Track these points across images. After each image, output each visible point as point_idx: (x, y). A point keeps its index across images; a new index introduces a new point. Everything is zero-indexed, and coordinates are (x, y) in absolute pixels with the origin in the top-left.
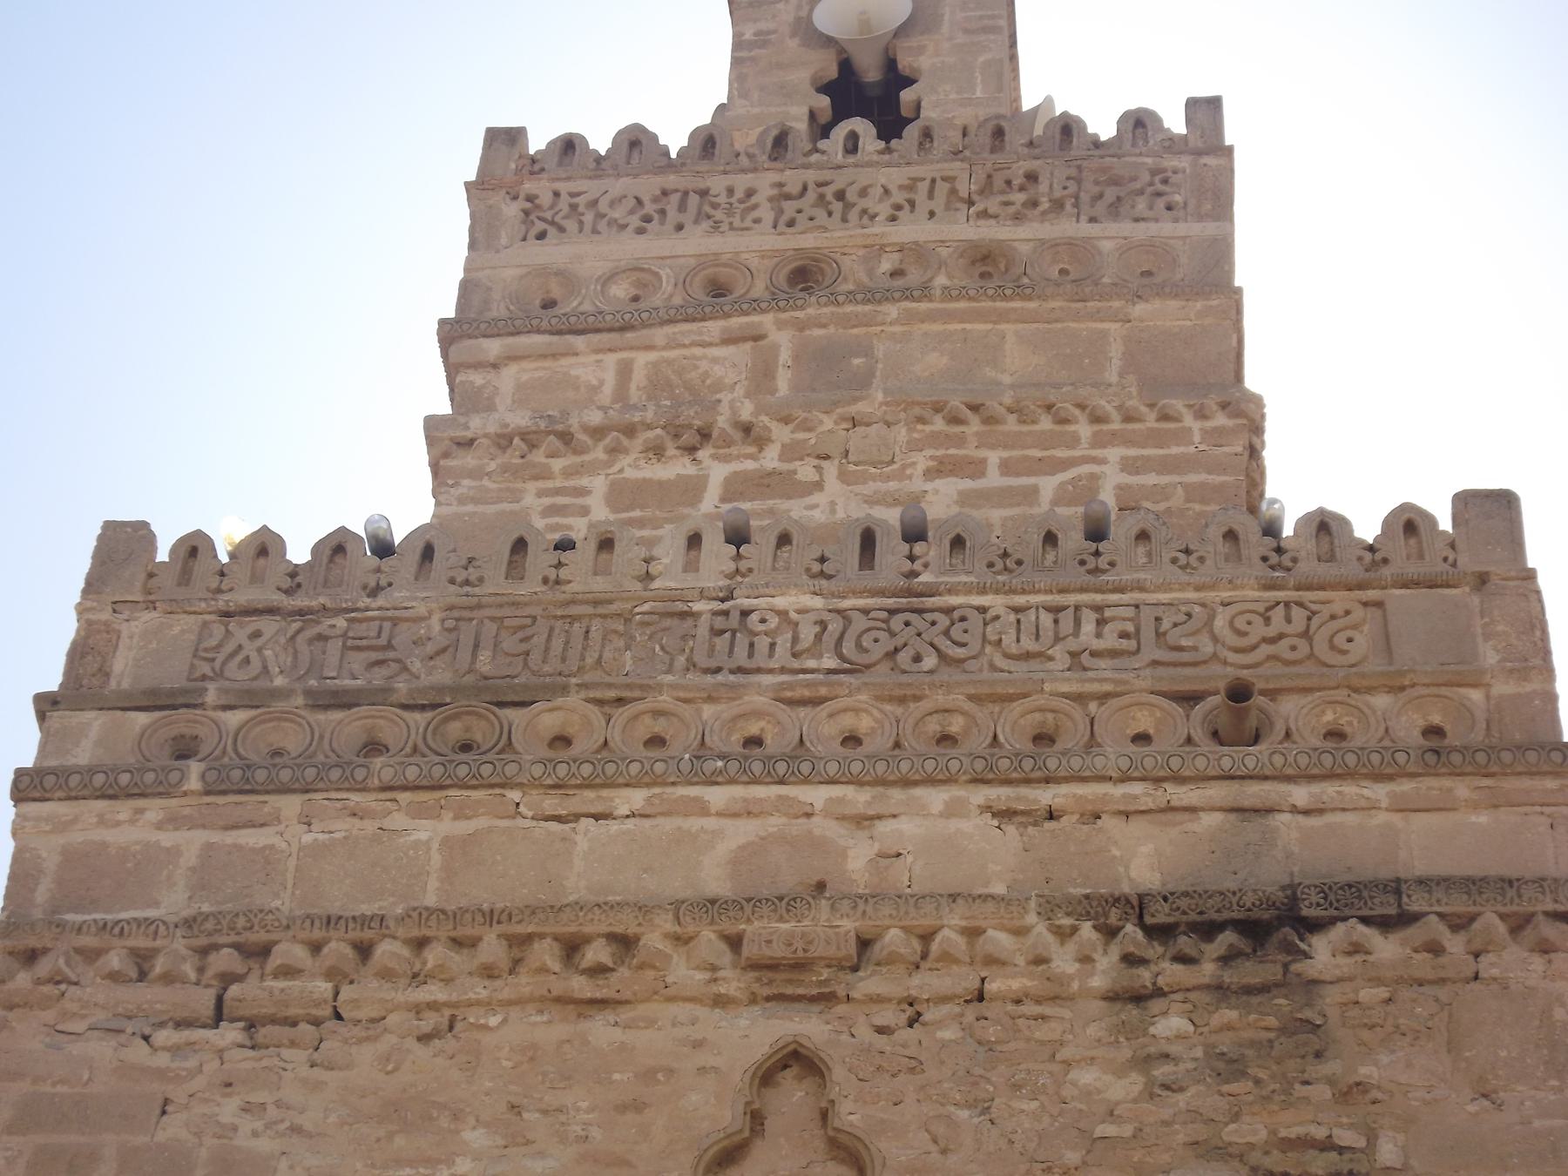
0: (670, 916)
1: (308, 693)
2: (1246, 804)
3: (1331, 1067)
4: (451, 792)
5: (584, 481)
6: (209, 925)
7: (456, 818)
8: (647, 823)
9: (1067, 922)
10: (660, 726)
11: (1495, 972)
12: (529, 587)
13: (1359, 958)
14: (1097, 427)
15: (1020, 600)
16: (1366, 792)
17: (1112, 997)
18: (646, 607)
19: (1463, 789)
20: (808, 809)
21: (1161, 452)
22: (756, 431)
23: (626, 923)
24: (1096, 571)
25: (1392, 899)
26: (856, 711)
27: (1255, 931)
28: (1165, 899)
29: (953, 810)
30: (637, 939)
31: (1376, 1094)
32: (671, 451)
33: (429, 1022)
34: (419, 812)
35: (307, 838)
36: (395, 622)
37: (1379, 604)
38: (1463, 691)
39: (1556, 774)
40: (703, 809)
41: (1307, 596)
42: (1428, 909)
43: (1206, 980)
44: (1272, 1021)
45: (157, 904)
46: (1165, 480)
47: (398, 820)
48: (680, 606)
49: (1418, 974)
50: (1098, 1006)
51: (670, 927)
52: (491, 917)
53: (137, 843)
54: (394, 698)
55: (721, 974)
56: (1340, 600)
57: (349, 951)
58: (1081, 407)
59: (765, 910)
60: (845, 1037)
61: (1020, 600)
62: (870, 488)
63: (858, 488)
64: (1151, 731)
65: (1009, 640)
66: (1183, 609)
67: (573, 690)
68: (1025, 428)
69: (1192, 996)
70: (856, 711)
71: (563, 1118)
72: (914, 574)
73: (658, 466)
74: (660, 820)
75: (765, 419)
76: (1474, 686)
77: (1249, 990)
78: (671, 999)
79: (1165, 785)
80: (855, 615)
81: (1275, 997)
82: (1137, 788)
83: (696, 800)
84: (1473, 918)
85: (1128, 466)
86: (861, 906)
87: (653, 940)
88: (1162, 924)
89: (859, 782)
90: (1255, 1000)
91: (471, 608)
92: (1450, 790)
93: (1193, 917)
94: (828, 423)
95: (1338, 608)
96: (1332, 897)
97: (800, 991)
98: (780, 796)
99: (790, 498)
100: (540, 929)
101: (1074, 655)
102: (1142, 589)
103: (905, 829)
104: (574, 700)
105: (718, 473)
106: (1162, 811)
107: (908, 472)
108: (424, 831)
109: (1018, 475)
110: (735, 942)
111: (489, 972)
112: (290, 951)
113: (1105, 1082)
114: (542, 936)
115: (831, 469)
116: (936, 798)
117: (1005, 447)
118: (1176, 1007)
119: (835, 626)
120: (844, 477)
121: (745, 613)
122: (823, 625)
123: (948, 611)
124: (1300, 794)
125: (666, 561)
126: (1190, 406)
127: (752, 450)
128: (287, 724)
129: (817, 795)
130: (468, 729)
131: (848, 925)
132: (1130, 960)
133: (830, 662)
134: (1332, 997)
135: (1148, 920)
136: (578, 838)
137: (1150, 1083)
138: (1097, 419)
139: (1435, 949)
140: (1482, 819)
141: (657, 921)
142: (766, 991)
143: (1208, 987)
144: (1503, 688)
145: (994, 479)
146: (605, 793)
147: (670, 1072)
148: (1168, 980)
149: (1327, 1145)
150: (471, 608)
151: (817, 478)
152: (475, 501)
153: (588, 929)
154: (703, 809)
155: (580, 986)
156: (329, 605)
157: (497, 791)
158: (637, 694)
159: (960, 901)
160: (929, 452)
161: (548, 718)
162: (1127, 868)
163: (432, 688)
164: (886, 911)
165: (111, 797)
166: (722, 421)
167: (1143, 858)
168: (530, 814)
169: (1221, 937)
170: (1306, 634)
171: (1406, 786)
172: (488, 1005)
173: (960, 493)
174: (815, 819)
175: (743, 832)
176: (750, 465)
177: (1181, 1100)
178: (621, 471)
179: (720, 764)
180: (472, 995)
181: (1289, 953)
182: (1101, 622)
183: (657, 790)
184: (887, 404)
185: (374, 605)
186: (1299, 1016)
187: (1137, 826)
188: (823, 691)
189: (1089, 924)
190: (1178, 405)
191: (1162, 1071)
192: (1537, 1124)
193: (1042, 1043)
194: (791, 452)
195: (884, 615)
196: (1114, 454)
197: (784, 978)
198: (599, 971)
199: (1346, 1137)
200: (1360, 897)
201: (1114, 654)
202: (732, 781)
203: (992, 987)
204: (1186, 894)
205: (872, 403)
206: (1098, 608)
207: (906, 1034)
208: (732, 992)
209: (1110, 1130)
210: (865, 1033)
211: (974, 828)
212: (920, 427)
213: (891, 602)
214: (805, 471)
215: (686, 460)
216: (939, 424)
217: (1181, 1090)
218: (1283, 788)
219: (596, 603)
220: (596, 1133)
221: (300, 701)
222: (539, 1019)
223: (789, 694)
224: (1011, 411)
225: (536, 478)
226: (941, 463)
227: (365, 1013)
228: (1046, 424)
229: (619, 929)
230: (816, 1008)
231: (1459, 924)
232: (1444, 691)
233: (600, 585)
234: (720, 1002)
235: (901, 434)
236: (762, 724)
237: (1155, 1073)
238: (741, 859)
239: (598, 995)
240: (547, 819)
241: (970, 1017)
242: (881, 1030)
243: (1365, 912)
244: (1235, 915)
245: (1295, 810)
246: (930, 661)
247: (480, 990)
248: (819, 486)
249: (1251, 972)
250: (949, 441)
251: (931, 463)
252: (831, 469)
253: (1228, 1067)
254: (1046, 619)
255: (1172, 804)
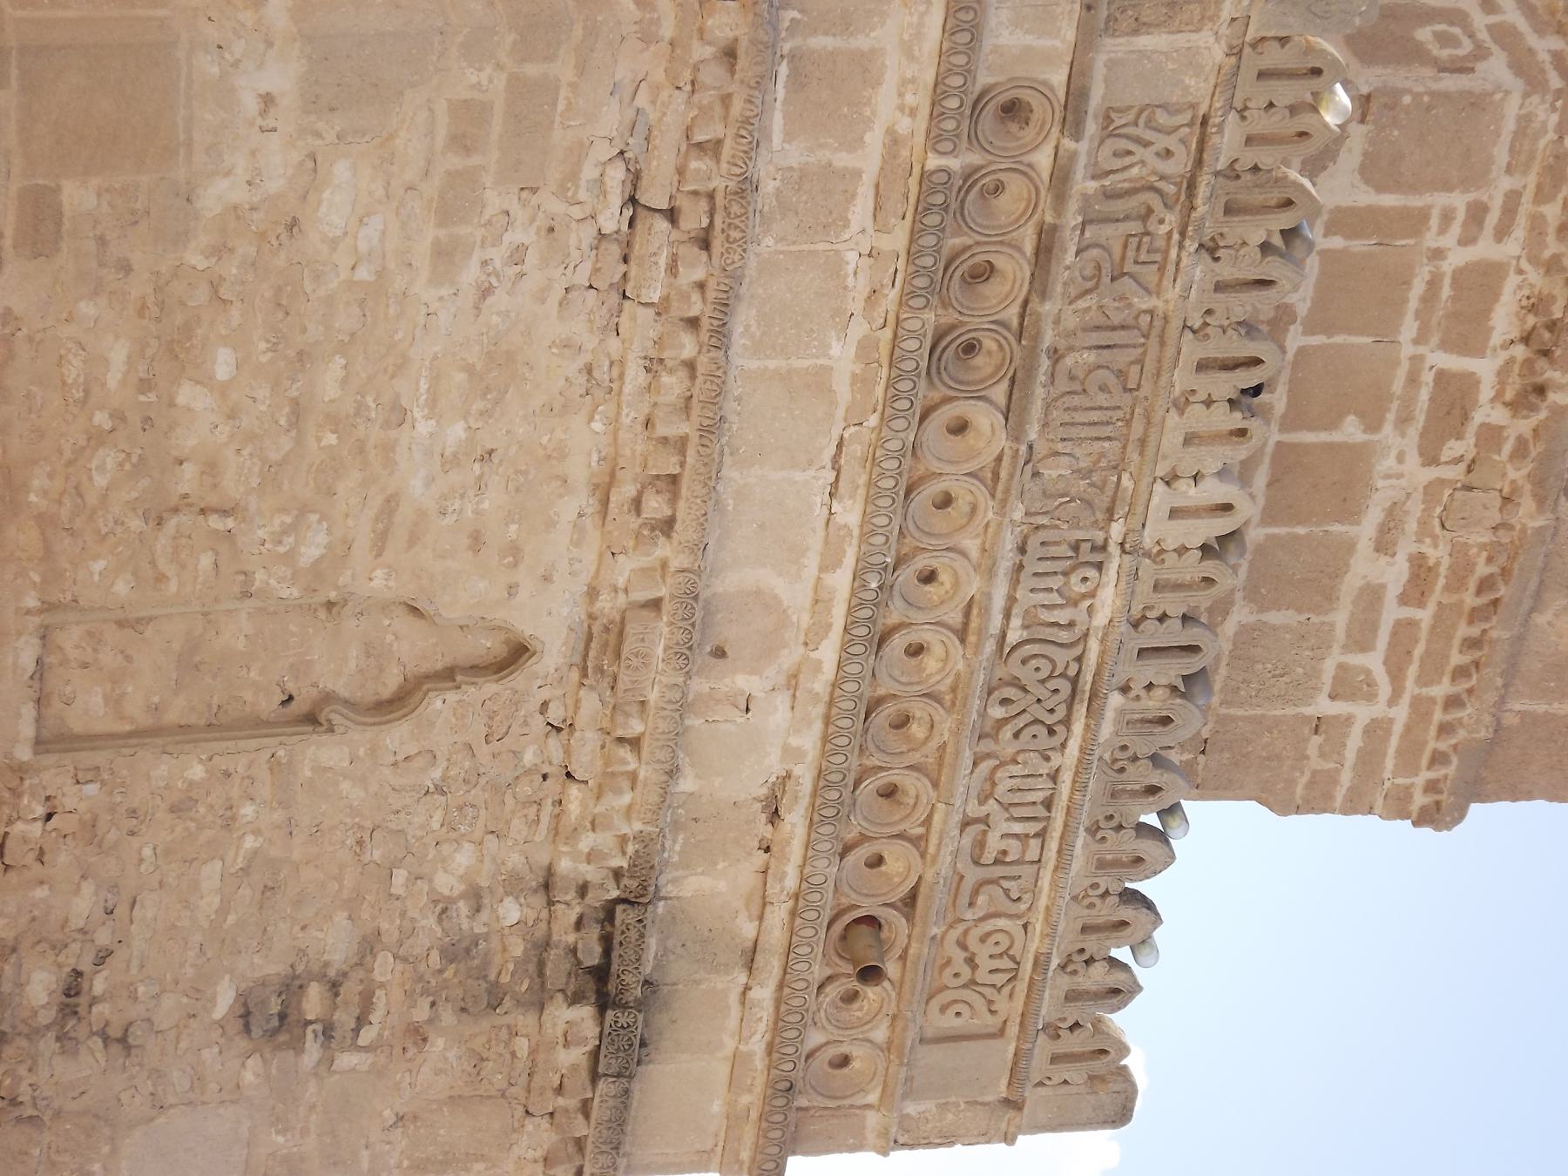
0: (686, 565)
1: (1054, 229)
2: (758, 957)
3: (448, 1017)
4: (884, 372)
5: (1520, 232)
6: (735, 209)
7: (854, 376)
8: (821, 523)
9: (630, 849)
10: (961, 506)
11: (530, 1128)
12: (1182, 378)
13: (561, 1040)
14: (1440, 701)
15: (1066, 778)
16: (758, 1037)
17: (550, 871)
18: (1126, 482)
19: (751, 1099)
20: (811, 647)
21: (1391, 751)
22: (1533, 398)
23: (684, 530)
24: (1094, 830)
25: (614, 1070)
26: (945, 660)
27: (601, 973)
28: (640, 921)
29: (790, 753)
30: (669, 536)
31: (412, 1051)
32: (1531, 320)
33: (601, 373)
34: (866, 348)
35: (852, 257)
36: (1162, 269)
37: (1001, 1033)
38: (879, 1090)
39: (753, 1160)
40: (829, 563)
41: (1022, 987)
42: (598, 1093)
43: (555, 937)
44: (505, 979)
45: (789, 137)
46: (1350, 754)
47: (859, 328)
48: (1120, 511)
49: (537, 1078)
50: (543, 859)
51: (674, 564)
52: (711, 430)
53: (874, 113)
54: (1035, 298)
55: (622, 596)
56: (1011, 1007)
57: (693, 313)
58: (1470, 691)
59: (680, 637)
60: (539, 682)
61: (1066, 778)
62: (1416, 508)
63: (1418, 495)
64: (883, 868)
65: (1016, 770)
66: (1026, 897)
67: (1015, 446)
68: (1456, 643)
69: (543, 926)
70: (945, 660)
71: (471, 493)
72: (1125, 690)
73: (1514, 308)
74: (821, 533)
75: (1543, 415)
76: (881, 1098)
77: (541, 965)
78: (601, 555)
79: (791, 903)
80: (1077, 651)
81: (531, 978)
82: (791, 882)
83: (838, 563)
84: (587, 1116)
85: (1377, 730)
86: (670, 707)
87: (663, 549)
88: (628, 902)
89: (835, 685)
90: (532, 968)
91: (1162, 337)
92: (750, 1091)
93: (617, 938)
94: (1517, 474)
95: (1001, 1004)
96: (622, 1032)
97: (592, 654)
98: (830, 625)
99: (1422, 435)
100: (688, 466)
101: (985, 820)
102: (1056, 868)
103: (776, 715)
104: (1002, 441)
105: (1485, 368)
106: (764, 897)
107: (1428, 540)
108: (841, 355)
109: (1394, 634)
110: (655, 604)
111: (648, 423)
112: (695, 269)
113: (458, 865)
114: (682, 464)
115: (1456, 473)
116: (809, 741)
117: (1433, 627)
118: (532, 915)
119: (1064, 636)
120: (1442, 482)
121: (1099, 566)
122: (1071, 624)
123: (1067, 722)
124: (764, 994)
125: (1192, 491)
126: (1446, 777)
127: (1509, 395)
128: (1023, 206)
129: (828, 653)
130: (990, 353)
131: (653, 697)
132: (583, 890)
133: (1013, 637)
134: (525, 1020)
135: (619, 908)
136: (811, 473)
137: (453, 900)
138: (1453, 702)
139: (560, 1090)
140: (717, 1107)
141: (681, 556)
142: (596, 629)
143: (550, 936)
144: (872, 1119)
145: (1392, 612)
146: (862, 492)
147: (515, 565)
148: (559, 913)
149: (362, 1021)
150: (1162, 337)
151: (1443, 459)
152: (1520, 134)
153: (682, 505)
154: (829, 563)
155: (625, 491)
156: (1194, 215)
157: (880, 408)
158: (999, 495)
159: (665, 778)
160: (1446, 562)
161: (986, 420)
162: (702, 873)
163: (1038, 333)
164: (663, 726)
165: (936, 85)
166: (1552, 375)
167: (712, 887)
168: (846, 436)
169: (598, 949)
170: (973, 982)
171: (759, 1062)
172: (614, 422)
173: (1383, 586)
174: (802, 649)
175: (794, 595)
176: (1486, 392)
177: (430, 921)
178: (1520, 272)
179: (874, 585)
180: (625, 411)
181: (575, 993)
182: (1023, 838)
183: (856, 532)
184: (1524, 530)
185: (1184, 254)
186: (507, 998)
187: (755, 880)
188: (972, 638)
189: (625, 865)
190: (1451, 770)
191: (463, 908)
192: (365, 1154)
193: (508, 822)
194: (1491, 436)
195: (1072, 672)
196: (1401, 714)
197: (603, 647)
198: (637, 504)
199: (367, 1036)
200: (618, 1050)
201: (980, 844)
202: (853, 594)
203: (574, 791)
204: (642, 936)
205: (1527, 515)
206: (1042, 835)
207: (538, 723)
208: (598, 605)
209: (400, 876)
210: (545, 694)
211: (774, 765)
212: (1485, 554)
213: (1088, 678)
214: (1462, 447)
215: (1515, 334)
216: (1482, 569)
217: (440, 920)
218: (772, 984)
219: (1143, 442)
220: (449, 520)
221: (1049, 219)
222: (595, 457)
223: (975, 611)
224: (1484, 631)
225: (1539, 187)
226: (1430, 569)
227: (624, 321)
228: (1457, 658)
229: (678, 527)
230: (577, 659)
231: (585, 1108)
232: (879, 1079)
233: (1171, 439)
234: (592, 593)
235: (1482, 537)
236: (948, 586)
237: (461, 904)
238: (765, 601)
239: (612, 505)
240: (840, 446)
241: (546, 769)
242: (545, 706)
243: (603, 1051)
244: (614, 967)
245: (747, 988)
246: (998, 712)
247: (631, 416)
248: (1430, 458)
249: (557, 969)
250: (1457, 581)
251: (1431, 563)
252: (1456, 473)
253: (457, 951)
254: (1038, 796)
255: (769, 908)
